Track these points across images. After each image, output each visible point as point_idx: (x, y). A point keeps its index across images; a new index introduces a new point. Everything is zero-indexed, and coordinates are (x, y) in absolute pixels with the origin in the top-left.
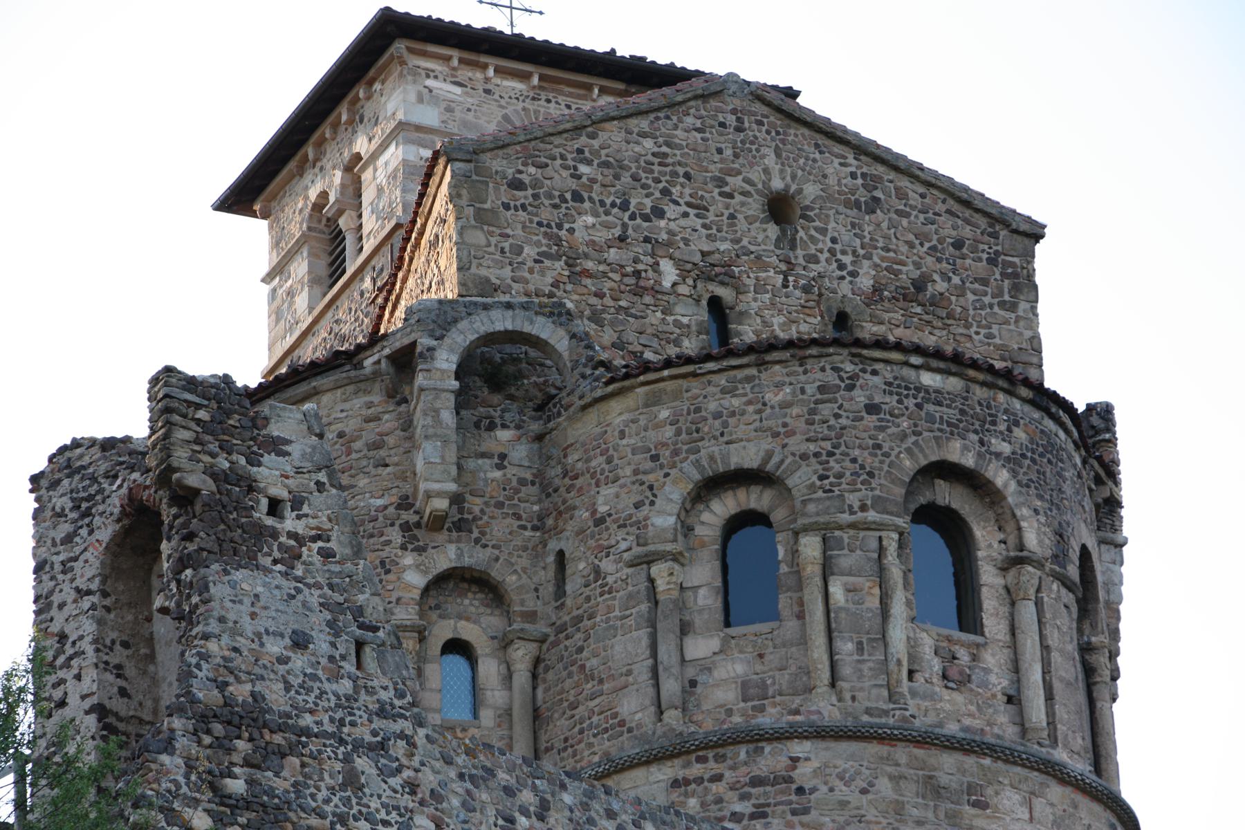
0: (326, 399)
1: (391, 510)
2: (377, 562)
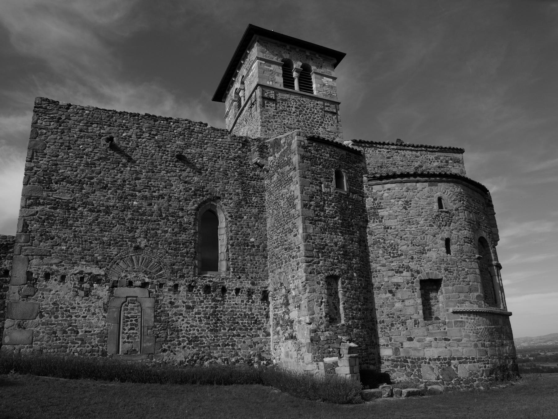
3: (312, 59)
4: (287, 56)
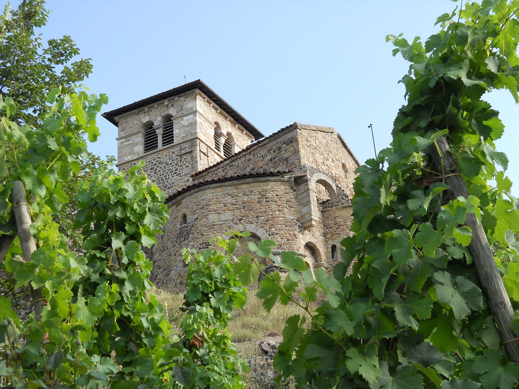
0: (271, 184)
1: (295, 221)
2: (293, 234)
3: (173, 106)
4: (145, 119)
